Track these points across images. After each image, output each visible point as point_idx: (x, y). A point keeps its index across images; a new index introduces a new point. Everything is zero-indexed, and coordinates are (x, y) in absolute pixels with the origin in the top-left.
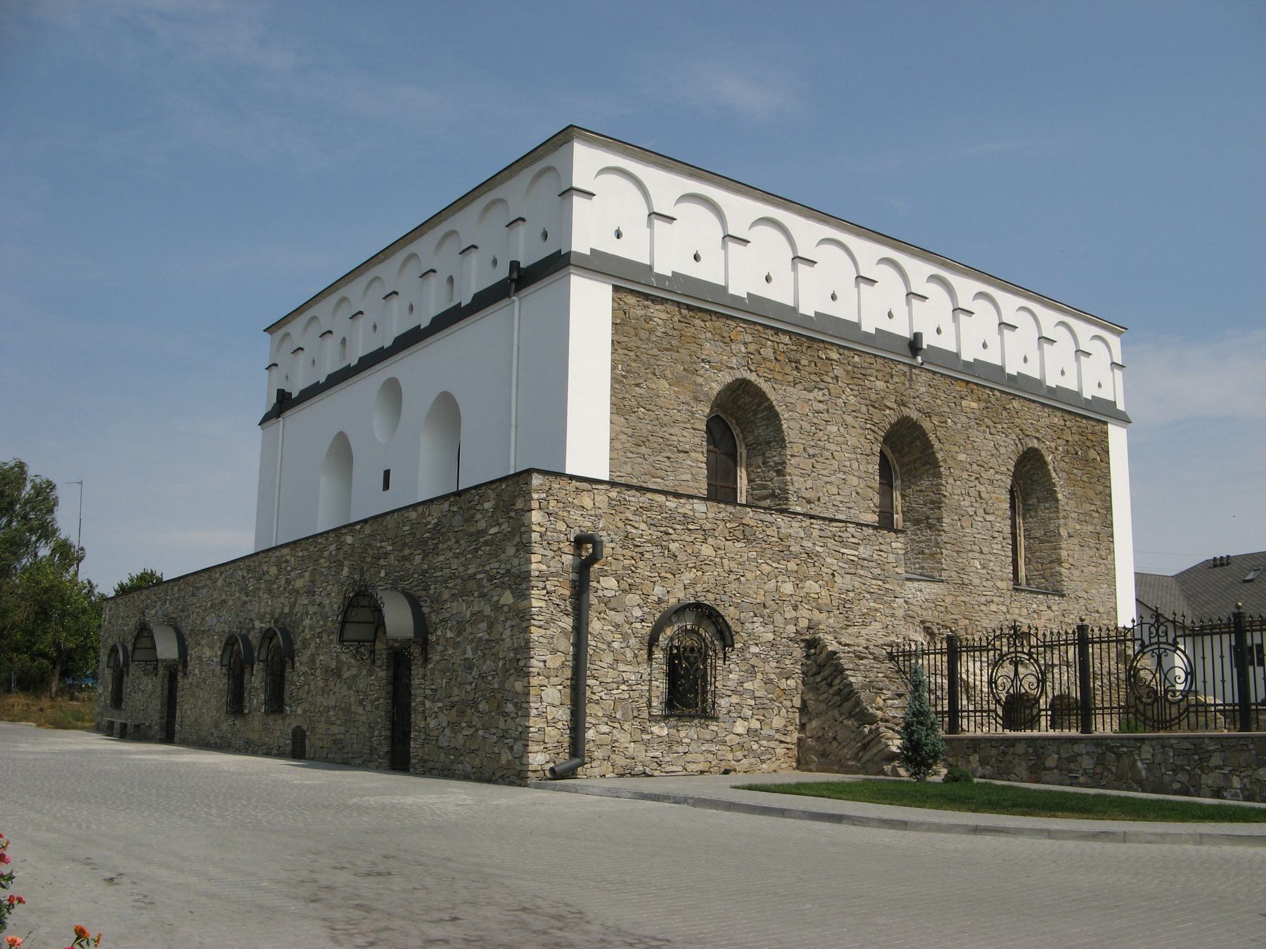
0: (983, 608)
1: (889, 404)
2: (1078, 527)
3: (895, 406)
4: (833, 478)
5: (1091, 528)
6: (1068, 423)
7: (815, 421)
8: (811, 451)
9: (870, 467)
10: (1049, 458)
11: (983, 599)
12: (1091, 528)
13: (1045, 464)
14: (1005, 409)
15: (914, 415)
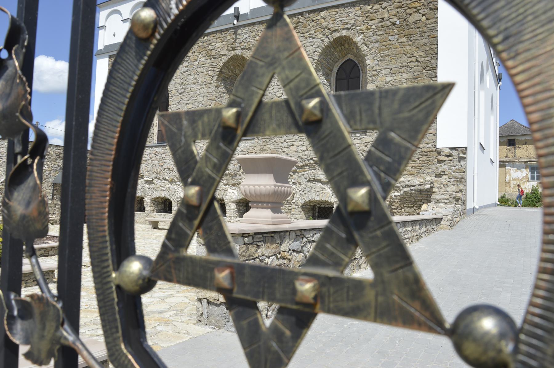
0: (285, 150)
1: (222, 53)
2: (389, 79)
3: (227, 52)
4: (190, 101)
5: (405, 76)
6: (383, 6)
7: (182, 77)
8: (180, 92)
9: (210, 90)
10: (358, 39)
11: (285, 144)
12: (405, 76)
13: (355, 43)
14: (313, 21)
15: (239, 52)
